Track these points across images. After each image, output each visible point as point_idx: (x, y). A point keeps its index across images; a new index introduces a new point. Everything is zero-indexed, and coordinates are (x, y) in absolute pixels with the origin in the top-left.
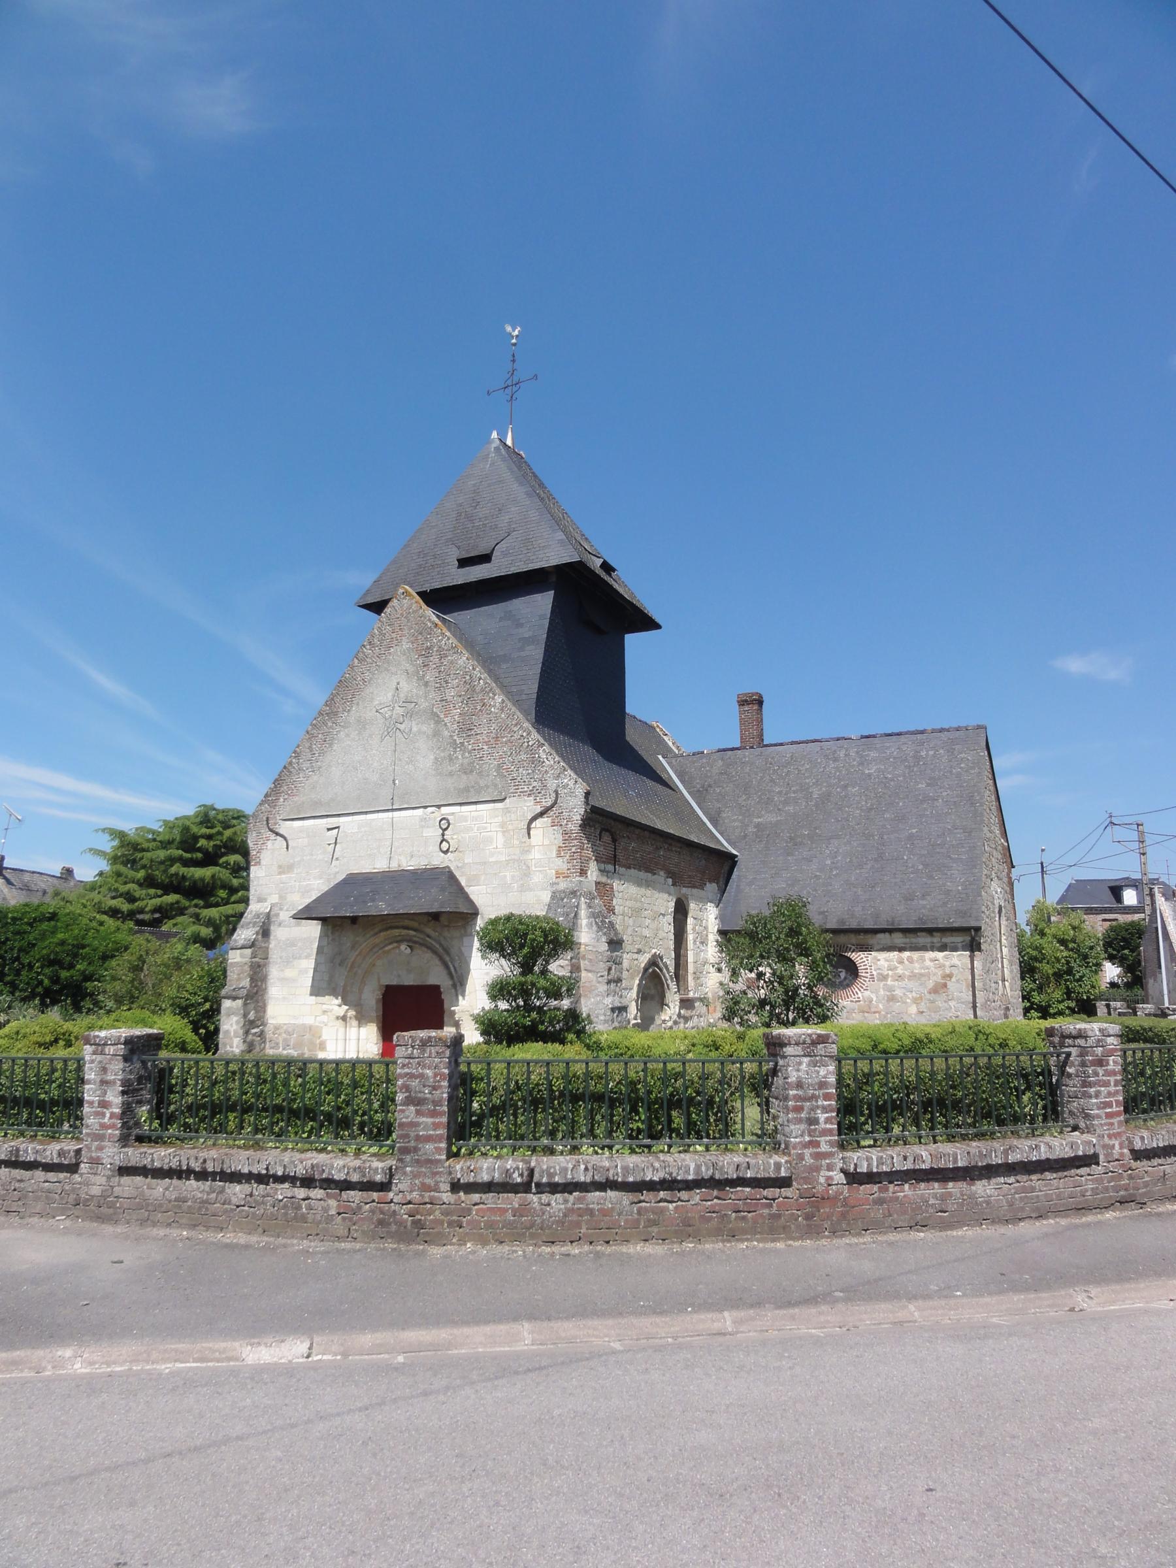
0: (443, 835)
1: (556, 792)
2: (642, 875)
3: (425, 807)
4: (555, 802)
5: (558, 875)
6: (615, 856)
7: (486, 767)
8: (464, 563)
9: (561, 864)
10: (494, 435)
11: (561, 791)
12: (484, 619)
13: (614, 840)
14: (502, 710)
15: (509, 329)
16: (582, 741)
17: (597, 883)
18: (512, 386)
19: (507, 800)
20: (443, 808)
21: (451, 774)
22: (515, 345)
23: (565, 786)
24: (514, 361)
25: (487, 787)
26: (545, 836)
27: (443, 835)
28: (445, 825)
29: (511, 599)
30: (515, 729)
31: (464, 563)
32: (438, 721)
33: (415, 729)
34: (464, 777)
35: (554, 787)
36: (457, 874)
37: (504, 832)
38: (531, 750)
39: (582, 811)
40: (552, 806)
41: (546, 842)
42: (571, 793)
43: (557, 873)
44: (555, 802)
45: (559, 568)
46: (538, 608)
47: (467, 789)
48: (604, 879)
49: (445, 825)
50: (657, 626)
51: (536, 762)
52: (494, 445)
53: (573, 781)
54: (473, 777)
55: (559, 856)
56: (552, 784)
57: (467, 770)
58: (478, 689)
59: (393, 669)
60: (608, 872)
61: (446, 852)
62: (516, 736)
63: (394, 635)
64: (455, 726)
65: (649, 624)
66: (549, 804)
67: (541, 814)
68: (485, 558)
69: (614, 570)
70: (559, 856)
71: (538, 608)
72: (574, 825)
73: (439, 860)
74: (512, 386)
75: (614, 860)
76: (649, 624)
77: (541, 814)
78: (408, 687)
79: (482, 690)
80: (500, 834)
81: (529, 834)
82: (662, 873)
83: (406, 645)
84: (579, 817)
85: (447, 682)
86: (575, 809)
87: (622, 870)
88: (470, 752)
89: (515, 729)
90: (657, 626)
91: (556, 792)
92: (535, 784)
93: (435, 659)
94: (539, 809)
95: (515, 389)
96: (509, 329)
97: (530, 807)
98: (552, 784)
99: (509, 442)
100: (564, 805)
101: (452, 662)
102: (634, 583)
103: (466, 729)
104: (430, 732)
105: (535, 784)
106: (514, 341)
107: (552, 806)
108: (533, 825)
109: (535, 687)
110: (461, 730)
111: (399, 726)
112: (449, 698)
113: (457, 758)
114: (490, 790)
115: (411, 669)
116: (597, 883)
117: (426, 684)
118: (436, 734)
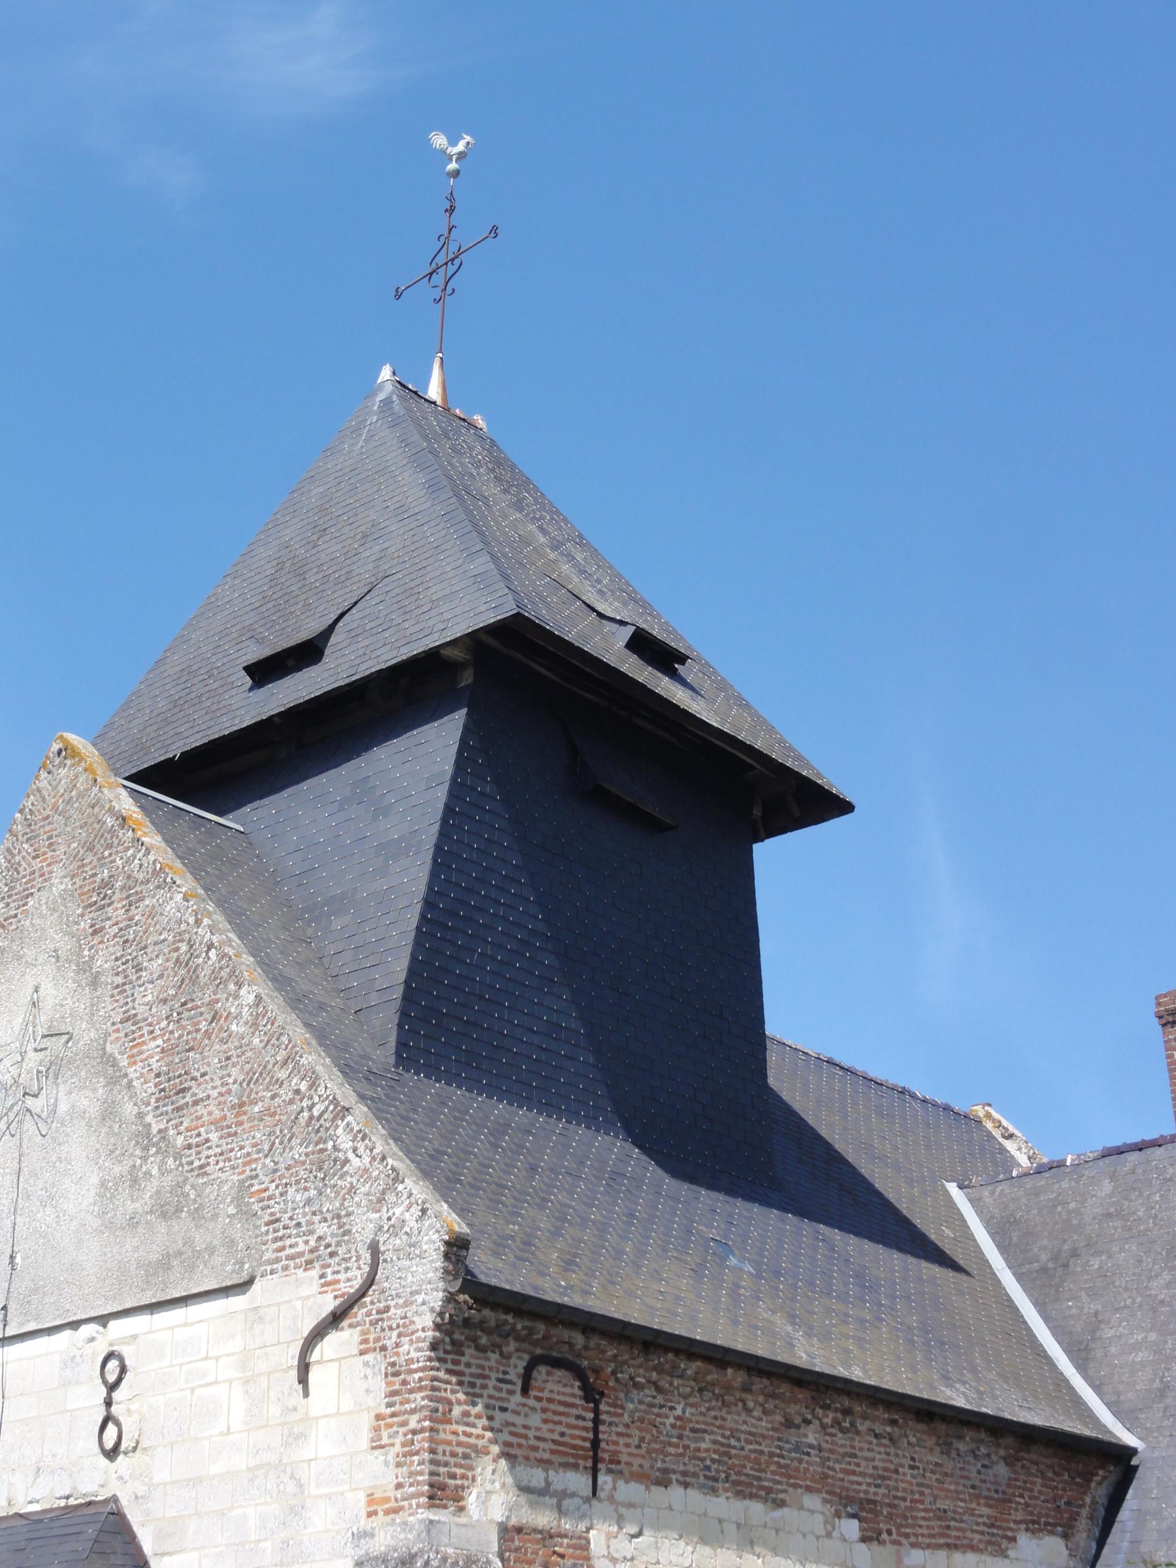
0: (108, 1403)
1: (374, 1249)
2: (724, 1505)
3: (75, 1325)
4: (370, 1282)
5: (374, 1505)
6: (596, 1443)
7: (211, 1192)
8: (263, 672)
9: (380, 1471)
10: (386, 373)
11: (388, 1246)
12: (300, 816)
13: (592, 1395)
14: (255, 1025)
15: (439, 140)
16: (591, 1121)
17: (508, 1532)
18: (445, 266)
19: (257, 1286)
20: (113, 1324)
21: (133, 1223)
22: (456, 174)
23: (396, 1229)
24: (451, 210)
25: (211, 1250)
26: (349, 1379)
27: (108, 1403)
28: (114, 1372)
29: (367, 748)
30: (282, 1074)
31: (263, 672)
32: (115, 1077)
33: (63, 1107)
34: (161, 1228)
35: (368, 1236)
36: (134, 1518)
37: (246, 1382)
38: (318, 1131)
39: (436, 1299)
40: (362, 1293)
41: (346, 1406)
42: (411, 1250)
43: (371, 1500)
44: (370, 1282)
45: (476, 641)
46: (422, 763)
47: (164, 1264)
48: (544, 1519)
49: (114, 1372)
50: (843, 807)
51: (327, 1165)
52: (381, 396)
53: (416, 1211)
54: (182, 1224)
55: (377, 1446)
56: (364, 1225)
57: (167, 1209)
58: (204, 975)
59: (29, 953)
60: (563, 1495)
61: (112, 1454)
62: (285, 1094)
63: (37, 864)
64: (151, 1087)
65: (813, 803)
66: (357, 1284)
67: (336, 1319)
68: (308, 653)
69: (682, 659)
70: (377, 1446)
71: (422, 763)
72: (415, 1351)
73: (94, 1479)
74: (445, 266)
75: (594, 1457)
76: (813, 803)
77: (336, 1319)
78: (58, 993)
79: (214, 974)
80: (237, 1388)
81: (303, 1380)
82: (812, 1501)
83: (59, 884)
84: (428, 1320)
85: (139, 969)
86: (419, 1291)
87: (628, 1490)
88: (178, 1156)
89: (282, 1074)
90: (843, 807)
91: (374, 1249)
92: (322, 1229)
93: (116, 911)
94: (329, 1304)
95: (451, 269)
96: (439, 140)
97: (302, 1298)
98: (364, 1225)
99: (434, 392)
100: (392, 1286)
101: (151, 914)
102: (751, 684)
103: (174, 1091)
104: (94, 1110)
105: (322, 1229)
106: (453, 166)
107: (362, 1293)
108: (315, 1356)
109: (399, 967)
110: (163, 1095)
111: (29, 1101)
112: (142, 1011)
113: (148, 1174)
114: (218, 1260)
115: (65, 944)
116: (508, 1532)
117: (94, 983)
118: (109, 1112)
